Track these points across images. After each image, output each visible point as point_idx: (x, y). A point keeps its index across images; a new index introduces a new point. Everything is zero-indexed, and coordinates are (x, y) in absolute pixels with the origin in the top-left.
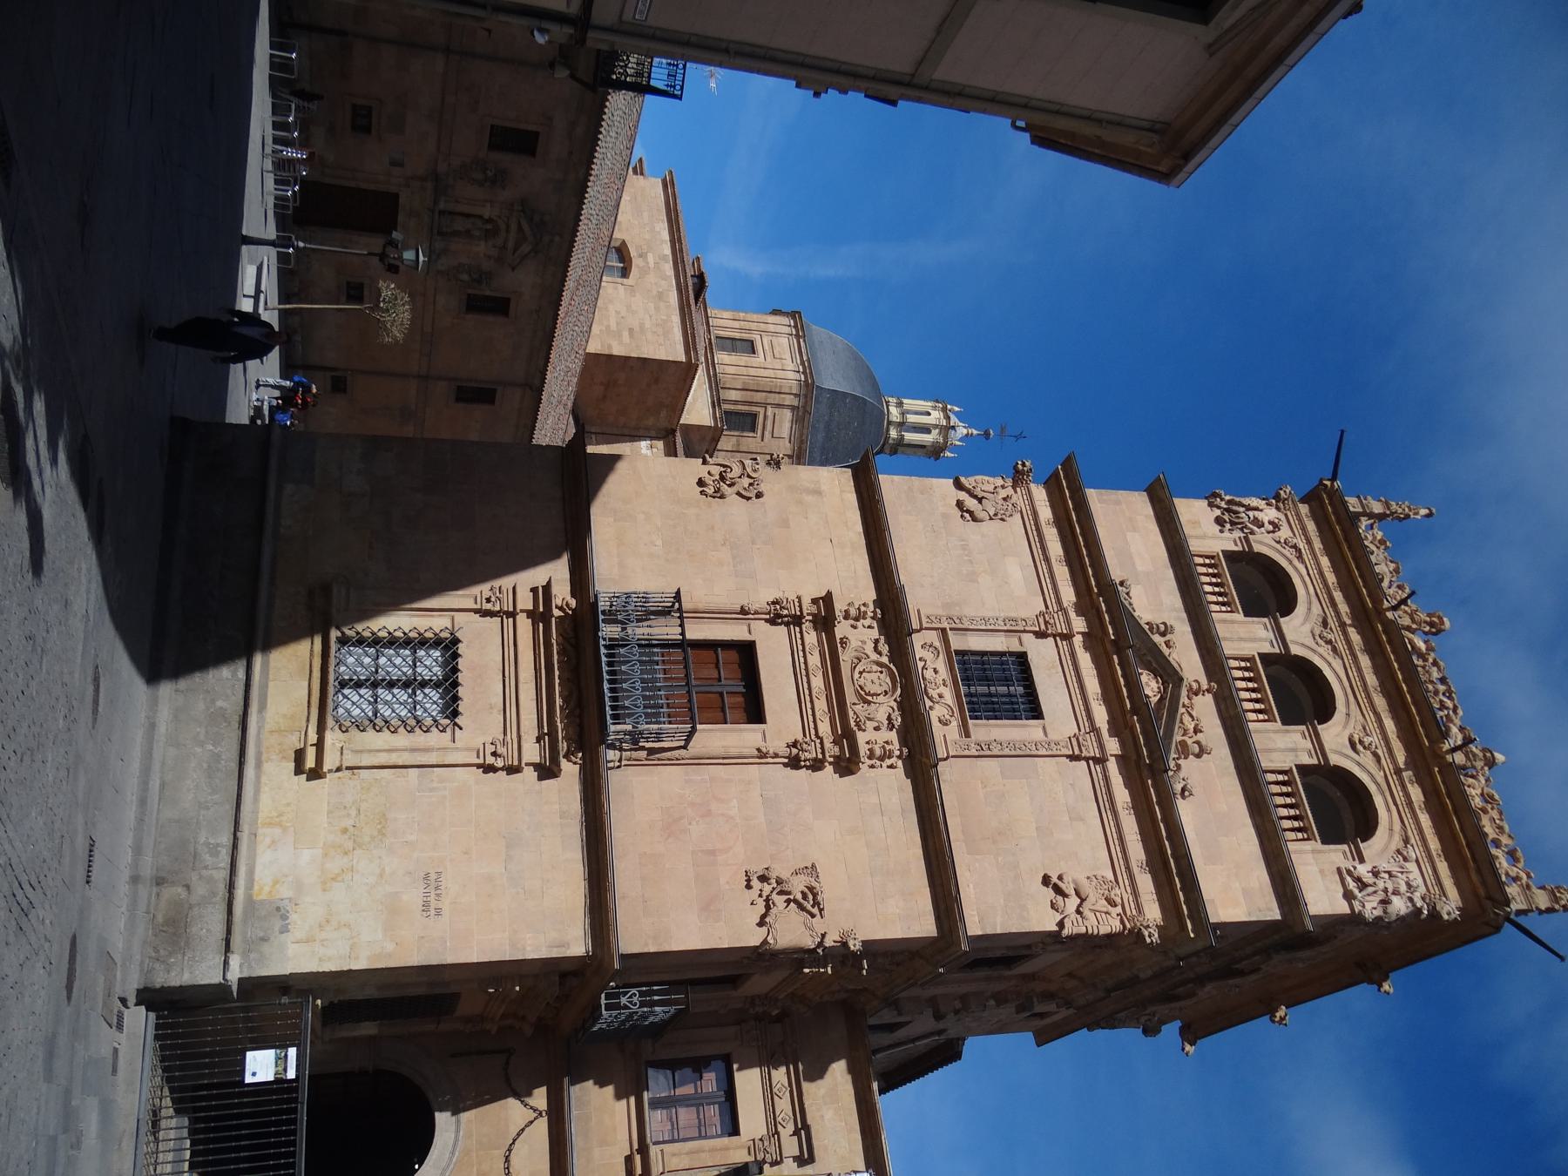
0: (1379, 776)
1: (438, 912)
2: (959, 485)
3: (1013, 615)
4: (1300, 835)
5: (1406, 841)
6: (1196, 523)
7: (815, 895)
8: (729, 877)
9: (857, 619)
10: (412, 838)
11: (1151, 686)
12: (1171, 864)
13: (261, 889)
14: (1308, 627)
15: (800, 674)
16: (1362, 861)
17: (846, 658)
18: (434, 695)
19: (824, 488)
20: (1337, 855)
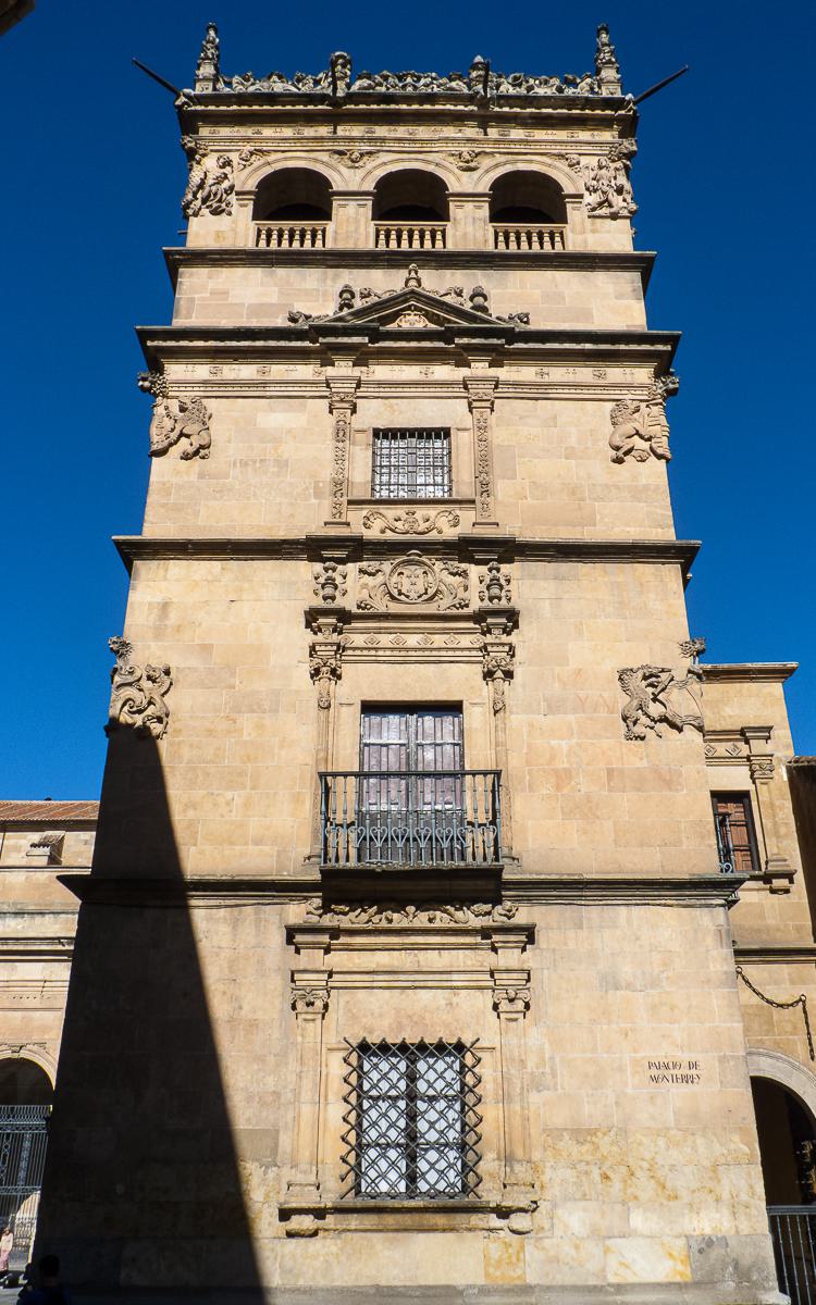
0: (499, 158)
1: (693, 1065)
2: (162, 453)
3: (330, 432)
4: (557, 239)
5: (561, 156)
6: (218, 235)
7: (651, 676)
8: (635, 758)
9: (336, 587)
11: (412, 322)
12: (604, 348)
13: (681, 1274)
14: (344, 170)
15: (402, 656)
16: (581, 196)
17: (381, 605)
18: (422, 1066)
19: (159, 599)
20: (576, 214)
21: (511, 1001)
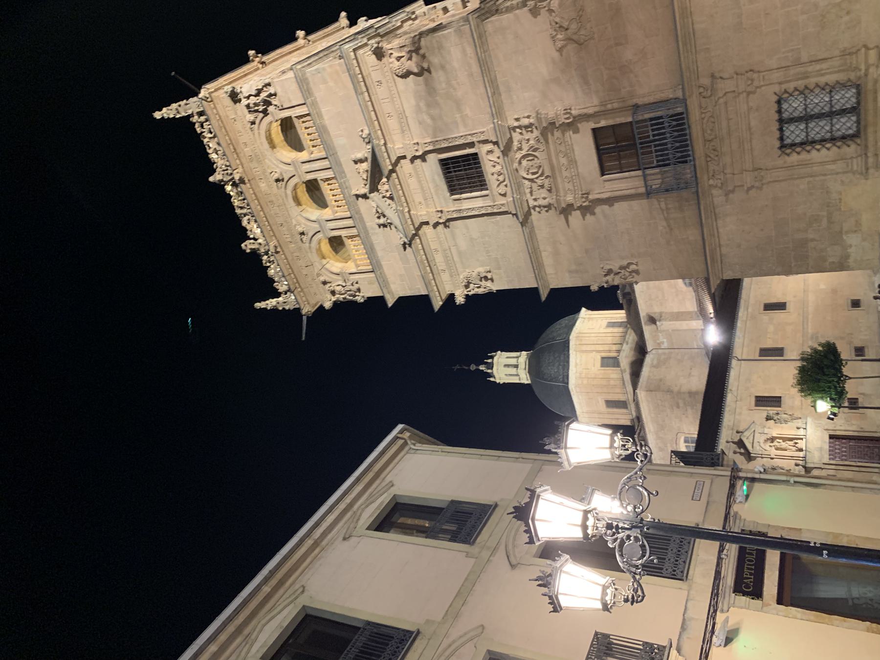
10: (805, 17)
19: (567, 275)
21: (752, 80)
